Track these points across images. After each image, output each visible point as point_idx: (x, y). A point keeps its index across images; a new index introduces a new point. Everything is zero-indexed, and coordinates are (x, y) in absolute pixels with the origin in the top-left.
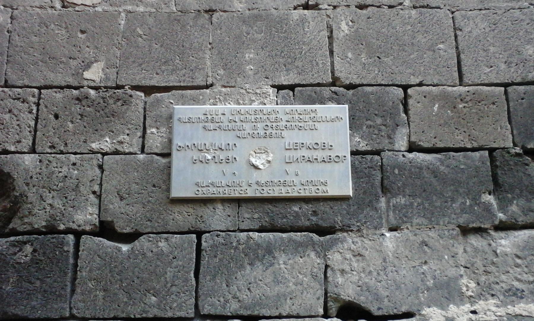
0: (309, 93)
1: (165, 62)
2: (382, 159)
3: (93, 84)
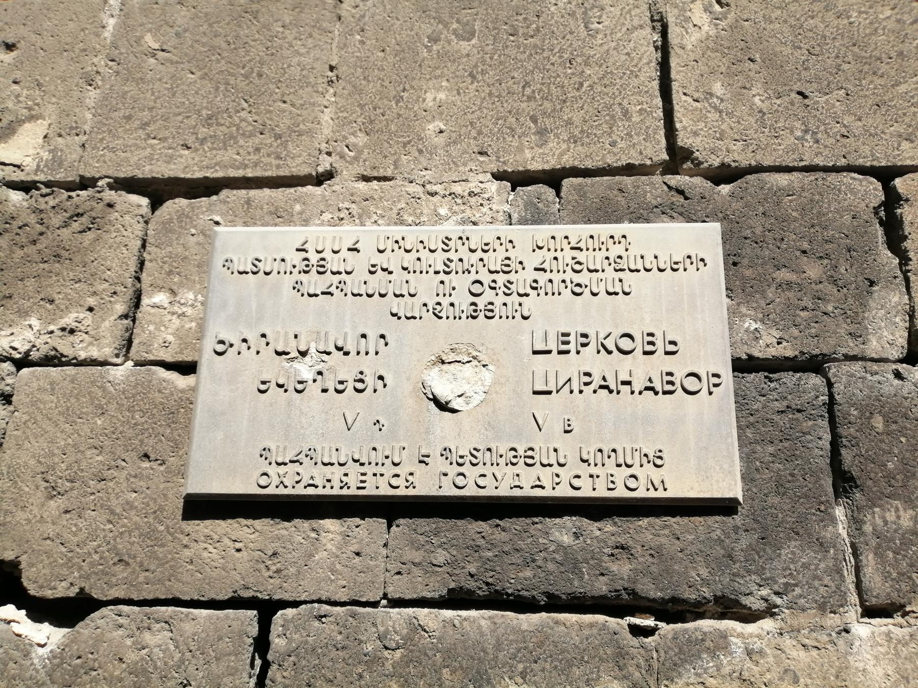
0: (601, 191)
1: (210, 117)
2: (830, 385)
3: (18, 176)
